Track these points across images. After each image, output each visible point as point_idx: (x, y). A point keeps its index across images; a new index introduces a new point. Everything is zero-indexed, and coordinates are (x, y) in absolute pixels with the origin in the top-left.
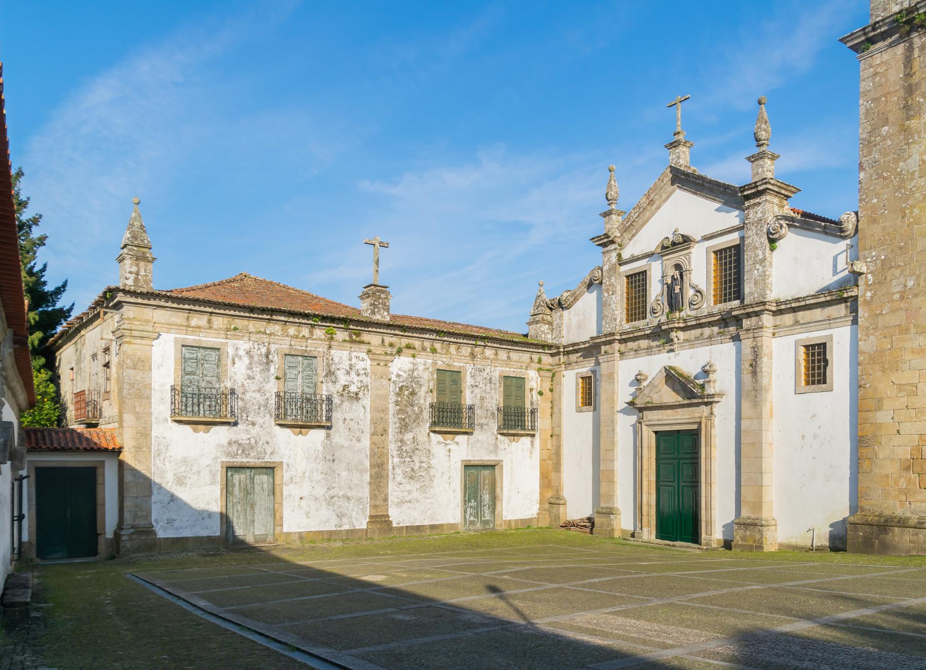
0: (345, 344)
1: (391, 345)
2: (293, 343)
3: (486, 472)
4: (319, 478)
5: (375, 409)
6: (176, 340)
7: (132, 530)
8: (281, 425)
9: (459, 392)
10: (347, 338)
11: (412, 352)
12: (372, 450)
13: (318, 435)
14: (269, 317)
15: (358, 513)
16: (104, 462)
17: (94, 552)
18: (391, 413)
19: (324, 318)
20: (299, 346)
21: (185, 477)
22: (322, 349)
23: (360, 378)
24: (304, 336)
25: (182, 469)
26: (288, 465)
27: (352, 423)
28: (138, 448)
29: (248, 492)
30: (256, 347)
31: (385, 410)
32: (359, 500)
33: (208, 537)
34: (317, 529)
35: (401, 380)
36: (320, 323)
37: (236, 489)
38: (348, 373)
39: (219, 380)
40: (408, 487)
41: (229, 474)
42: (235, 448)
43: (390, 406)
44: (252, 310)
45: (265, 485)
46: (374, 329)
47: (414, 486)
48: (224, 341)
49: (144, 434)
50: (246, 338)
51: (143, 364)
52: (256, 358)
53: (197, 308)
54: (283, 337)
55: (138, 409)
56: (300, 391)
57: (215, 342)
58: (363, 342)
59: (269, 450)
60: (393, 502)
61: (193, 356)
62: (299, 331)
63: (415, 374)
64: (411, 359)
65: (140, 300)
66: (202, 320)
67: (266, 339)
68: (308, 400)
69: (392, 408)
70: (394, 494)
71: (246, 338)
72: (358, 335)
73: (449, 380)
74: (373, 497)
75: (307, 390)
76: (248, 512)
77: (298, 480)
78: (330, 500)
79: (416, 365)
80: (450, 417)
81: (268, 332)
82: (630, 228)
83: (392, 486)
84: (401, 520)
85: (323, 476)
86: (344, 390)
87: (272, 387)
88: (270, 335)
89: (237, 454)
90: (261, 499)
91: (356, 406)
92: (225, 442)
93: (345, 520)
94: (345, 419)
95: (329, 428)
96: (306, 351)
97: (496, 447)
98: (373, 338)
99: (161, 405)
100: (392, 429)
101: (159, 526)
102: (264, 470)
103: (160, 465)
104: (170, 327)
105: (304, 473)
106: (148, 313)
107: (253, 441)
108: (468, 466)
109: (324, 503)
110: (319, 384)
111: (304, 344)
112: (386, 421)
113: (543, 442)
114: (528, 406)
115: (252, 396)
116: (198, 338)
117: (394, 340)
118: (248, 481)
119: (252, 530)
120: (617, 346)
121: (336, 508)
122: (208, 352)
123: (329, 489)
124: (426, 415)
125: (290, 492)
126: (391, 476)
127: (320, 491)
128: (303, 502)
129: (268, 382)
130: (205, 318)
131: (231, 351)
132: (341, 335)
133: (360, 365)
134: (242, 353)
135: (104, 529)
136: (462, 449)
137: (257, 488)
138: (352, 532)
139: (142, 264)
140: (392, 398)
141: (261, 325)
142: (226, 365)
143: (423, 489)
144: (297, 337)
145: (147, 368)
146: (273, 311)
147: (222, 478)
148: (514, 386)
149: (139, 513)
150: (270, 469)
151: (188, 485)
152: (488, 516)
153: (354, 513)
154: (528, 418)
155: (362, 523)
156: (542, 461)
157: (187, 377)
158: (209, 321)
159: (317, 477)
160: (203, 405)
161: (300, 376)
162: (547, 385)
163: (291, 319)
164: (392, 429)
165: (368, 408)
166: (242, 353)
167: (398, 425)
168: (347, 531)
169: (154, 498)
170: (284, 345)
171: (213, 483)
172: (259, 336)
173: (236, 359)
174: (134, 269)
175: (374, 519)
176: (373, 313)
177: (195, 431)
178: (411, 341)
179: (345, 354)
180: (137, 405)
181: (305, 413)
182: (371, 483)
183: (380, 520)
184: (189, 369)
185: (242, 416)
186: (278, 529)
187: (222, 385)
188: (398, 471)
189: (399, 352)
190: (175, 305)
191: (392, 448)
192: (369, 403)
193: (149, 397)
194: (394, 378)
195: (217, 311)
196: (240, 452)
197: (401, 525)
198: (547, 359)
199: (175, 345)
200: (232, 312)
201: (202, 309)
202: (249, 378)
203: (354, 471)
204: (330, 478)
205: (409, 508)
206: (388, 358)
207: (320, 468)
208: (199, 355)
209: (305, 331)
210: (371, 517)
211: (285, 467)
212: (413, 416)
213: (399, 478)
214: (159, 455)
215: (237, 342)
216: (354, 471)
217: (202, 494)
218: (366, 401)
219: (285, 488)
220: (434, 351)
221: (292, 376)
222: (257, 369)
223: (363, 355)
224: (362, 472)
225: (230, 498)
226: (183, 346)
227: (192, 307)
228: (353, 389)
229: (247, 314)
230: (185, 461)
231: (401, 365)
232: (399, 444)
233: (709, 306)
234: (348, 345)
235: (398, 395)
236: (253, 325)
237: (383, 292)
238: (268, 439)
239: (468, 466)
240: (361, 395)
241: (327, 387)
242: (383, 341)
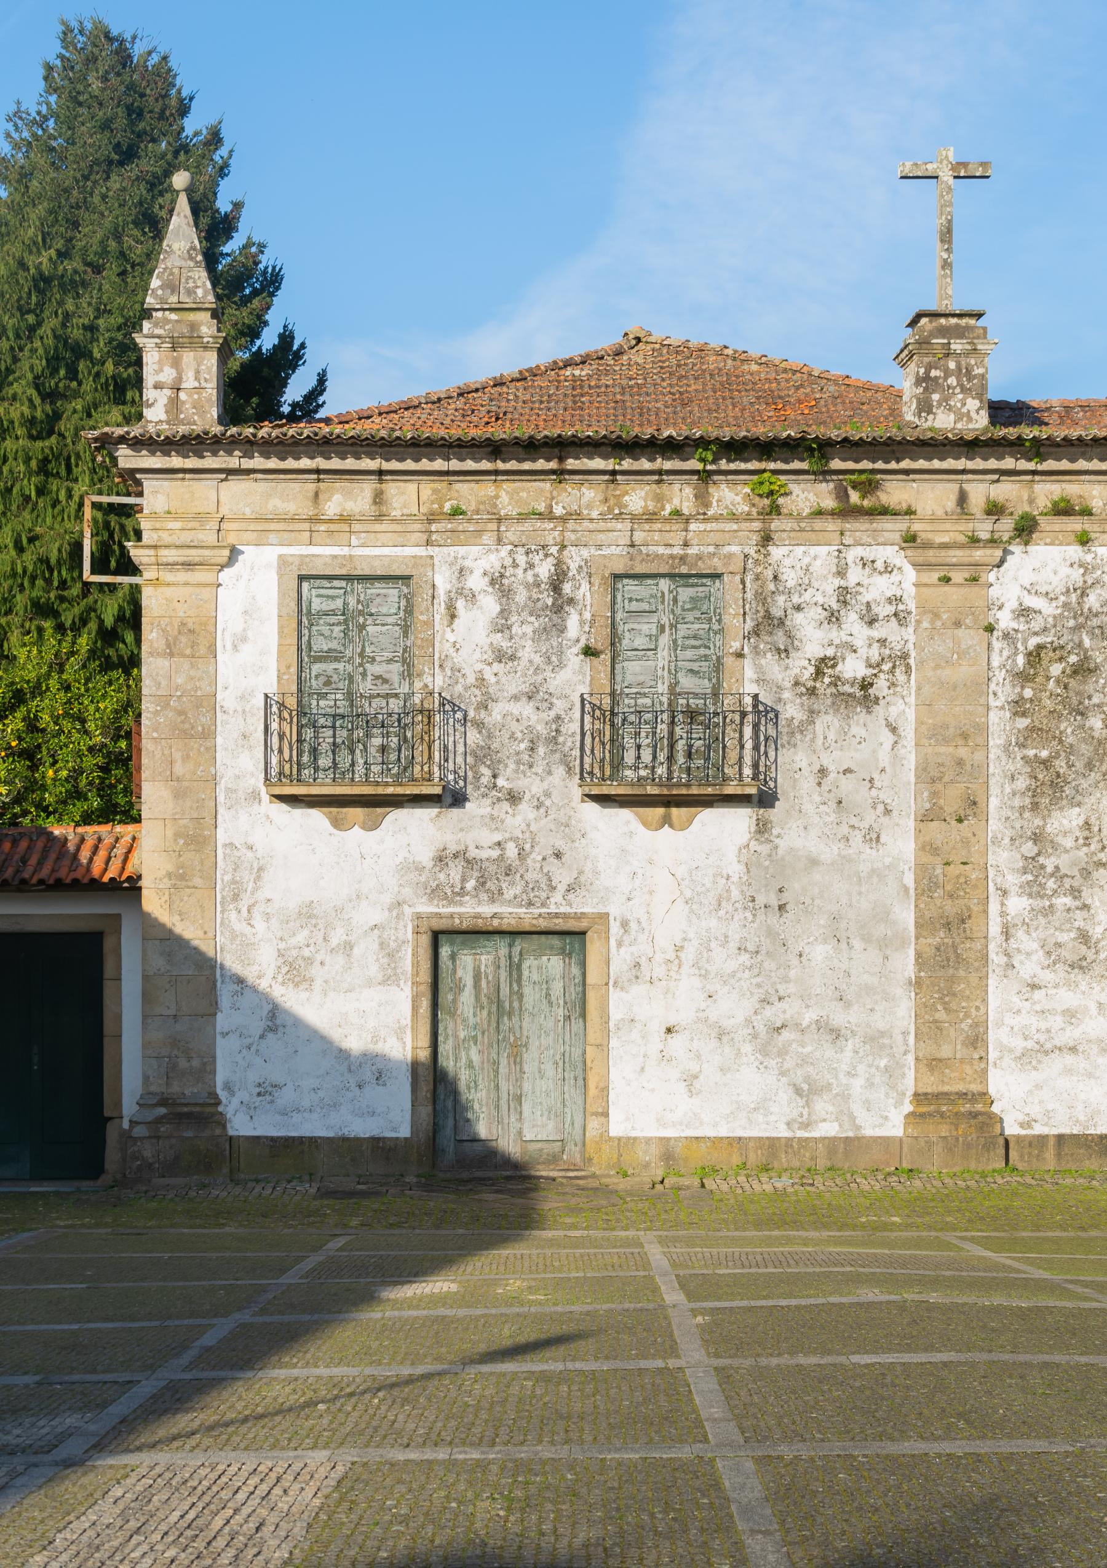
0: (818, 524)
1: (995, 510)
2: (639, 536)
4: (732, 965)
5: (932, 733)
6: (283, 561)
7: (162, 1111)
8: (603, 800)
10: (830, 503)
11: (1076, 524)
12: (921, 870)
13: (725, 829)
14: (553, 465)
15: (870, 1084)
16: (118, 917)
17: (93, 1167)
18: (996, 741)
19: (735, 448)
20: (662, 544)
21: (309, 961)
22: (740, 545)
23: (877, 633)
24: (677, 513)
25: (301, 937)
26: (625, 924)
27: (847, 785)
28: (180, 878)
29: (501, 1008)
30: (522, 559)
31: (972, 734)
32: (876, 1040)
33: (376, 1142)
34: (723, 1131)
35: (1036, 625)
36: (723, 464)
37: (467, 997)
38: (833, 618)
39: (409, 672)
40: (1066, 998)
41: (445, 951)
42: (455, 872)
43: (994, 717)
44: (495, 449)
45: (557, 987)
46: (922, 464)
48: (421, 551)
49: (198, 837)
50: (488, 538)
52: (521, 596)
53: (335, 463)
54: (604, 520)
55: (179, 769)
56: (663, 688)
57: (393, 559)
58: (885, 511)
59: (563, 877)
60: (1004, 1049)
61: (329, 611)
62: (659, 499)
63: (1093, 600)
64: (1075, 551)
65: (176, 462)
66: (356, 498)
67: (550, 533)
68: (692, 715)
69: (1000, 724)
70: (1009, 1020)
71: (488, 538)
72: (869, 486)
74: (929, 1028)
75: (687, 682)
76: (503, 1070)
77: (659, 971)
81: (558, 511)
83: (999, 995)
84: (1035, 1111)
85: (745, 958)
86: (819, 673)
87: (574, 679)
88: (563, 519)
89: (463, 892)
90: (541, 1029)
91: (860, 723)
92: (425, 857)
93: (822, 1106)
94: (823, 772)
95: (765, 799)
96: (683, 559)
98: (925, 495)
99: (241, 757)
100: (1001, 798)
101: (235, 1101)
102: (555, 941)
103: (239, 926)
104: (266, 526)
105: (679, 949)
107: (511, 851)
109: (747, 1048)
110: (729, 661)
111: (677, 538)
112: (980, 772)
115: (511, 714)
116: (345, 551)
117: (1006, 491)
118: (503, 975)
119: (514, 1125)
121: (789, 1063)
122: (378, 589)
123: (765, 1001)
125: (626, 1008)
126: (996, 958)
127: (734, 1008)
128: (676, 1042)
129: (561, 665)
130: (367, 488)
131: (443, 581)
132: (807, 495)
133: (878, 588)
134: (476, 582)
135: (118, 1104)
137: (531, 995)
138: (852, 1145)
139: (188, 357)
140: (1002, 691)
141: (535, 493)
142: (430, 624)
144: (651, 517)
145: (202, 650)
146: (561, 447)
147: (416, 965)
149: (183, 1063)
150: (571, 938)
151: (318, 984)
153: (858, 1084)
155: (887, 1118)
157: (317, 668)
158: (378, 498)
159: (724, 960)
160: (360, 749)
161: (665, 640)
163: (627, 464)
164: (1001, 798)
165: (908, 731)
166: (476, 582)
167: (1022, 783)
168: (831, 1143)
169: (222, 1021)
170: (612, 548)
171: (389, 979)
172: (527, 526)
173: (460, 604)
174: (168, 375)
176: (925, 407)
177: (337, 824)
178: (1072, 489)
179: (821, 556)
180: (177, 756)
181: (684, 760)
182: (918, 983)
183: (957, 1113)
184: (321, 645)
185: (477, 777)
186: (593, 1124)
187: (418, 685)
188: (1024, 941)
189: (1026, 530)
190: (273, 463)
191: (1003, 862)
192: (911, 714)
193: (209, 734)
194: (1005, 620)
195: (394, 465)
196: (470, 885)
197: (1038, 1130)
199: (281, 576)
200: (439, 464)
201: (350, 463)
202: (500, 656)
203: (857, 944)
204: (769, 965)
205: (1068, 1071)
206: (979, 554)
207: (735, 933)
208: (352, 601)
209: (681, 496)
210: (919, 1097)
211: (615, 929)
212: (1086, 750)
213: (1030, 967)
214: (236, 897)
215: (462, 550)
216: (857, 944)
217: (368, 1013)
218: (903, 706)
219: (614, 996)
221: (640, 642)
222: (524, 628)
223: (890, 554)
224: (886, 945)
225: (446, 1024)
226: (302, 578)
227: (321, 463)
228: (853, 668)
229: (485, 465)
230: (308, 914)
232: (1029, 848)
234: (832, 525)
235: (1023, 678)
236: (509, 496)
237: (960, 333)
238: (560, 844)
240: (881, 686)
241: (759, 669)
242: (962, 499)
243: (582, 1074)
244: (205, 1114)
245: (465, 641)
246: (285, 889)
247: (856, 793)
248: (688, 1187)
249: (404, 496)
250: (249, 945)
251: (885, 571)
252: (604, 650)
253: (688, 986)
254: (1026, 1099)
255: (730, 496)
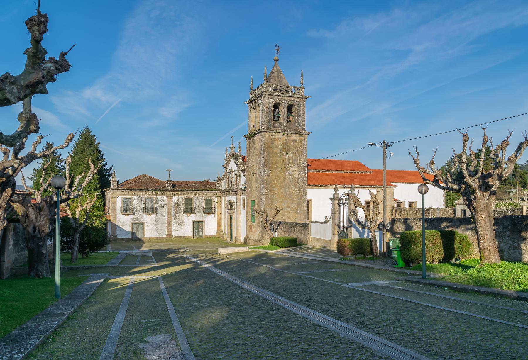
3: (200, 223)
5: (168, 209)
9: (192, 204)
13: (153, 216)
20: (149, 196)
28: (114, 220)
29: (137, 228)
47: (179, 227)
51: (115, 203)
54: (145, 195)
61: (125, 201)
69: (173, 208)
73: (188, 202)
74: (168, 229)
78: (157, 230)
79: (179, 198)
80: (189, 209)
82: (227, 164)
83: (173, 227)
87: (143, 206)
90: (140, 230)
97: (203, 217)
98: (168, 193)
100: (173, 214)
104: (120, 195)
106: (115, 192)
108: (194, 222)
113: (218, 215)
114: (213, 206)
115: (138, 208)
120: (226, 193)
124: (182, 210)
125: (147, 228)
132: (159, 193)
133: (164, 199)
136: (192, 218)
140: (173, 206)
141: (140, 193)
143: (181, 228)
148: (208, 202)
150: (143, 224)
152: (201, 234)
154: (213, 209)
155: (165, 236)
156: (218, 220)
159: (153, 225)
160: (127, 210)
162: (219, 200)
164: (173, 214)
170: (146, 196)
175: (168, 235)
181: (151, 211)
183: (170, 235)
189: (175, 195)
198: (219, 193)
213: (175, 225)
217: (129, 229)
218: (166, 207)
220: (184, 194)
222: (139, 202)
224: (165, 224)
228: (163, 205)
231: (175, 198)
233: (235, 187)
239: (194, 222)
243: (143, 233)
244: (116, 236)
245: (135, 203)
246: (122, 220)
247: (163, 213)
248: (151, 240)
249: (131, 193)
250: (119, 224)
251: (165, 198)
252: (145, 203)
253: (151, 227)
254: (174, 234)
255: (154, 193)
